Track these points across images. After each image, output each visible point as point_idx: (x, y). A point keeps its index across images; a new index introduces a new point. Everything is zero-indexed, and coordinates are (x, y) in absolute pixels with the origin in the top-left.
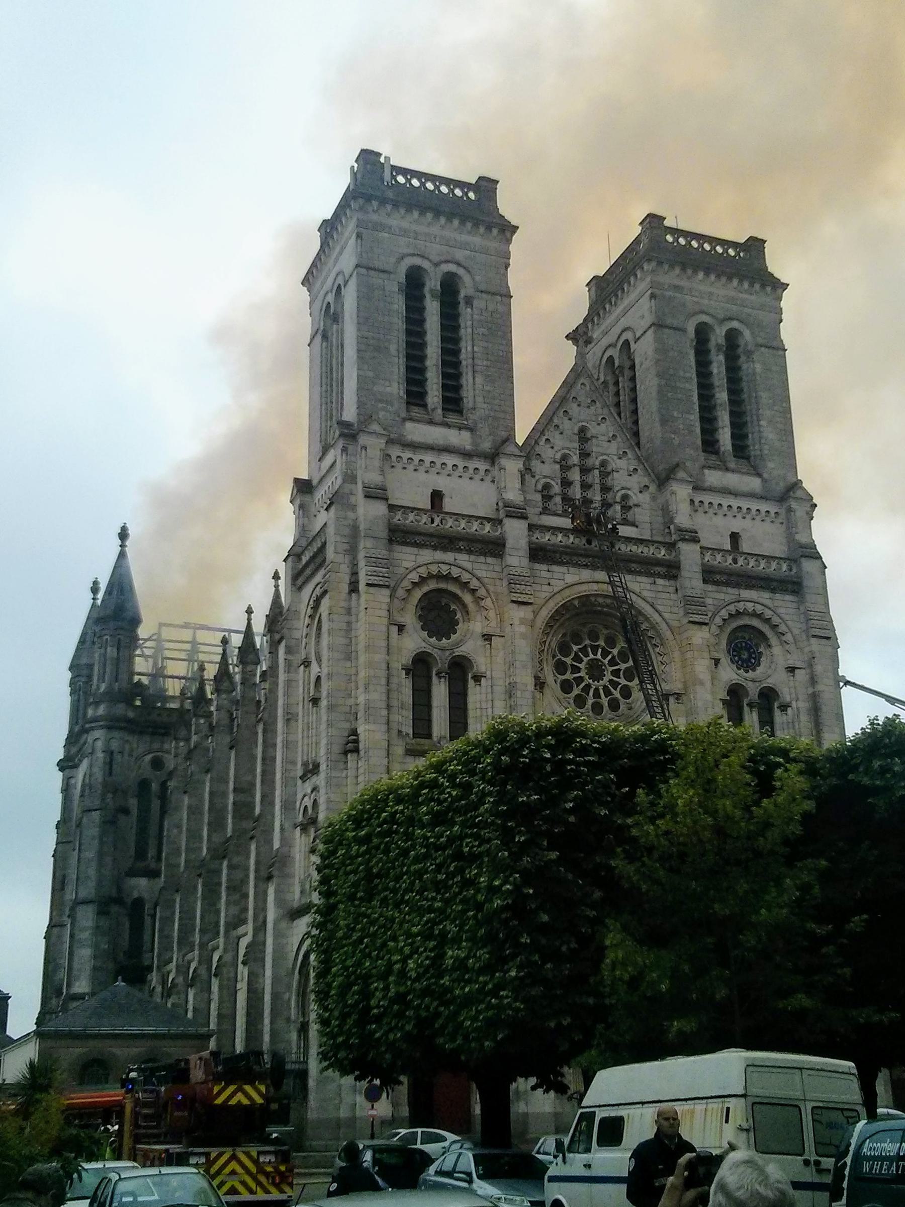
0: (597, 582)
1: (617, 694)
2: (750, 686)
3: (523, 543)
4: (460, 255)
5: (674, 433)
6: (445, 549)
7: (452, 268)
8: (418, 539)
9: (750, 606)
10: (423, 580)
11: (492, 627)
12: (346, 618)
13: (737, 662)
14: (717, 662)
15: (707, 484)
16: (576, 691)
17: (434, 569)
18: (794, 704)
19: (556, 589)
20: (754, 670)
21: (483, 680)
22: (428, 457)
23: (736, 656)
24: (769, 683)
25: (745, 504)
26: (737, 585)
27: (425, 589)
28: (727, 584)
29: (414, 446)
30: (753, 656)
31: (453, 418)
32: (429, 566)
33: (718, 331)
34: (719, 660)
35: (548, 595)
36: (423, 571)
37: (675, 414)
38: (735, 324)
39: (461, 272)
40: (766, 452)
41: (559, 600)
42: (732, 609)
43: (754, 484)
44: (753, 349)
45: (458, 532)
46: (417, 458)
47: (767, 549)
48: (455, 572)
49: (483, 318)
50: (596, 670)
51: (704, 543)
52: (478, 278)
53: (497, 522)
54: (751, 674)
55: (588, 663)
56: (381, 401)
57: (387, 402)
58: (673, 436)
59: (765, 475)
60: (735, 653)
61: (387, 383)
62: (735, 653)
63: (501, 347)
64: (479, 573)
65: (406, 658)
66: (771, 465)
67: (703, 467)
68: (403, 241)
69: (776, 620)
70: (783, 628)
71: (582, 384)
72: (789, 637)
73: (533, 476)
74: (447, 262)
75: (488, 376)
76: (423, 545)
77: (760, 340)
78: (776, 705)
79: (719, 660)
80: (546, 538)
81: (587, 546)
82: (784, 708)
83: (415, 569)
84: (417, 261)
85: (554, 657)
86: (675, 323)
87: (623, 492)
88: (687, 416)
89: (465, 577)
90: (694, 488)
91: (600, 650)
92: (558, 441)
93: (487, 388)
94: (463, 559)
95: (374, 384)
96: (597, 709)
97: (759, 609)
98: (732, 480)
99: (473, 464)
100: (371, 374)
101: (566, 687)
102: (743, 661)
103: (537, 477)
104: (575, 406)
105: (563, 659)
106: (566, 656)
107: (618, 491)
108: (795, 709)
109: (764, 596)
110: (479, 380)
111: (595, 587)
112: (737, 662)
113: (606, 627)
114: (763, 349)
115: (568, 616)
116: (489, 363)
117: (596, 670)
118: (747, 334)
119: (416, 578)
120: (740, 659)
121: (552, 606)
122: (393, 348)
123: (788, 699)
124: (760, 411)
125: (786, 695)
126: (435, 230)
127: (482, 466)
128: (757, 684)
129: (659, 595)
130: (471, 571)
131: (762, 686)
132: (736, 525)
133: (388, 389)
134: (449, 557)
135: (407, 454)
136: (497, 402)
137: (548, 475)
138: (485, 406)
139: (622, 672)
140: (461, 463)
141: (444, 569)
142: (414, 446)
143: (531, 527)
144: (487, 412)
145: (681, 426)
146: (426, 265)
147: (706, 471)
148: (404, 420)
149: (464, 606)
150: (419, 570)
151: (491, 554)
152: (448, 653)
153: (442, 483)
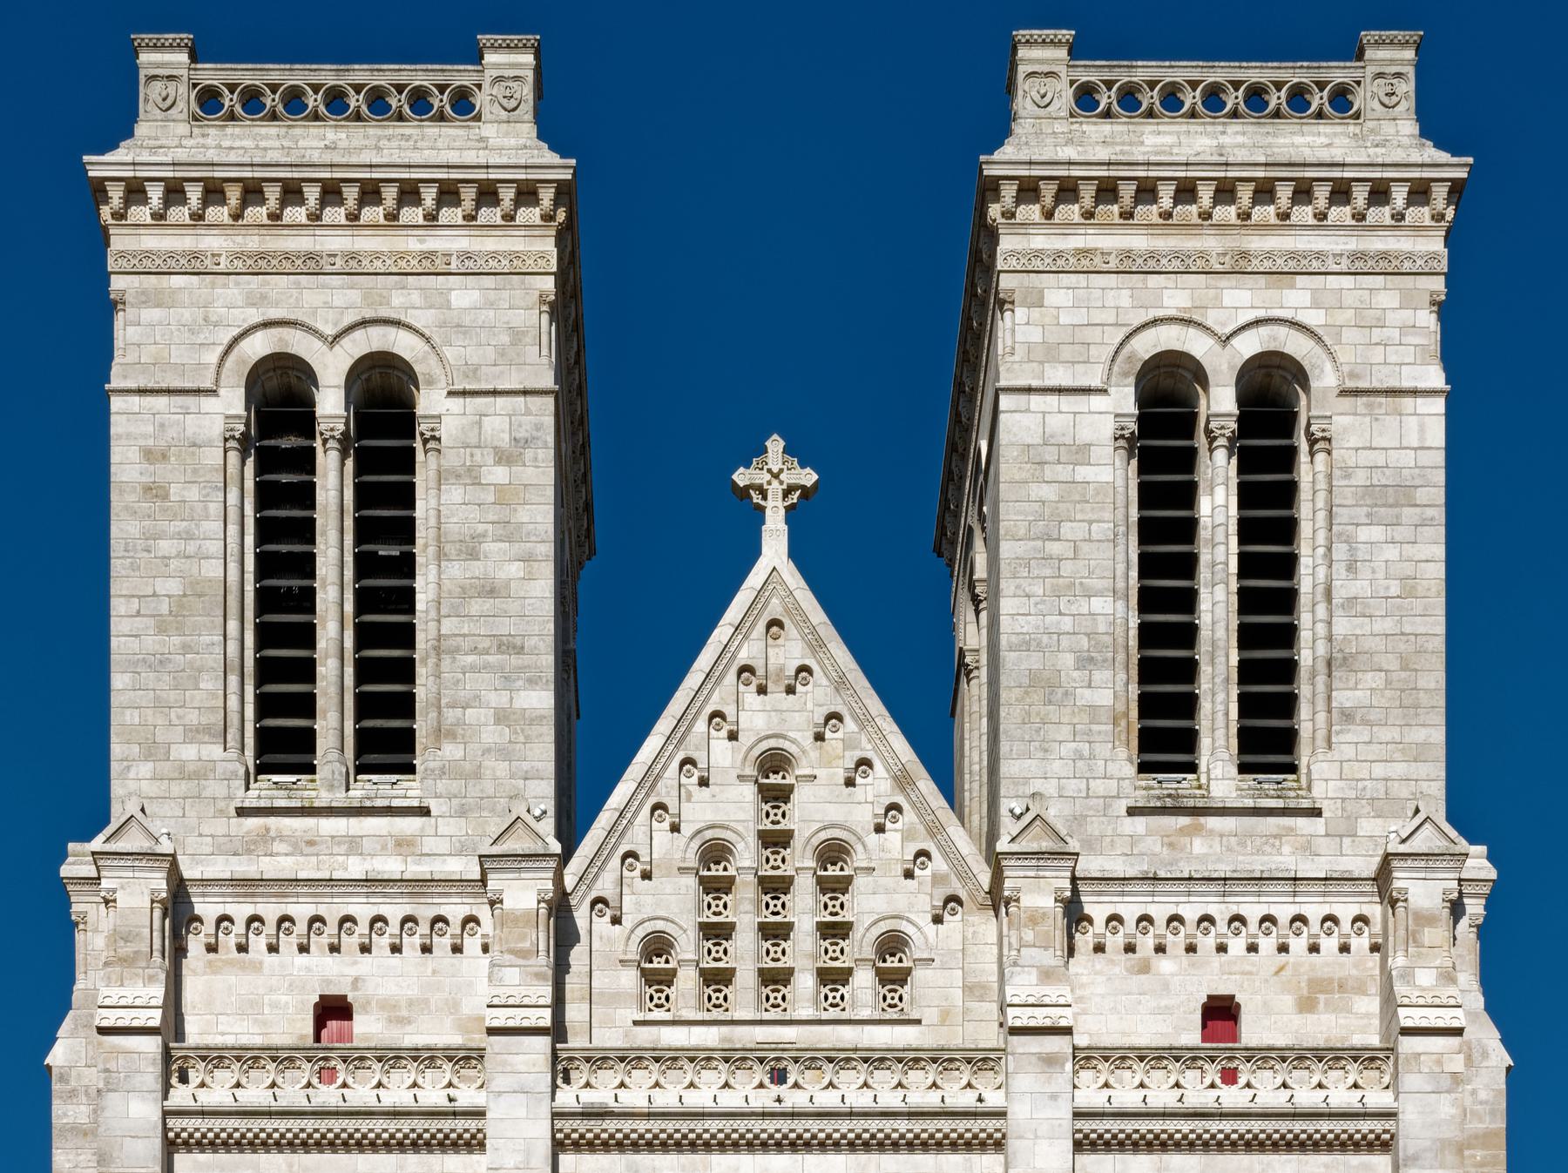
68: (233, 290)
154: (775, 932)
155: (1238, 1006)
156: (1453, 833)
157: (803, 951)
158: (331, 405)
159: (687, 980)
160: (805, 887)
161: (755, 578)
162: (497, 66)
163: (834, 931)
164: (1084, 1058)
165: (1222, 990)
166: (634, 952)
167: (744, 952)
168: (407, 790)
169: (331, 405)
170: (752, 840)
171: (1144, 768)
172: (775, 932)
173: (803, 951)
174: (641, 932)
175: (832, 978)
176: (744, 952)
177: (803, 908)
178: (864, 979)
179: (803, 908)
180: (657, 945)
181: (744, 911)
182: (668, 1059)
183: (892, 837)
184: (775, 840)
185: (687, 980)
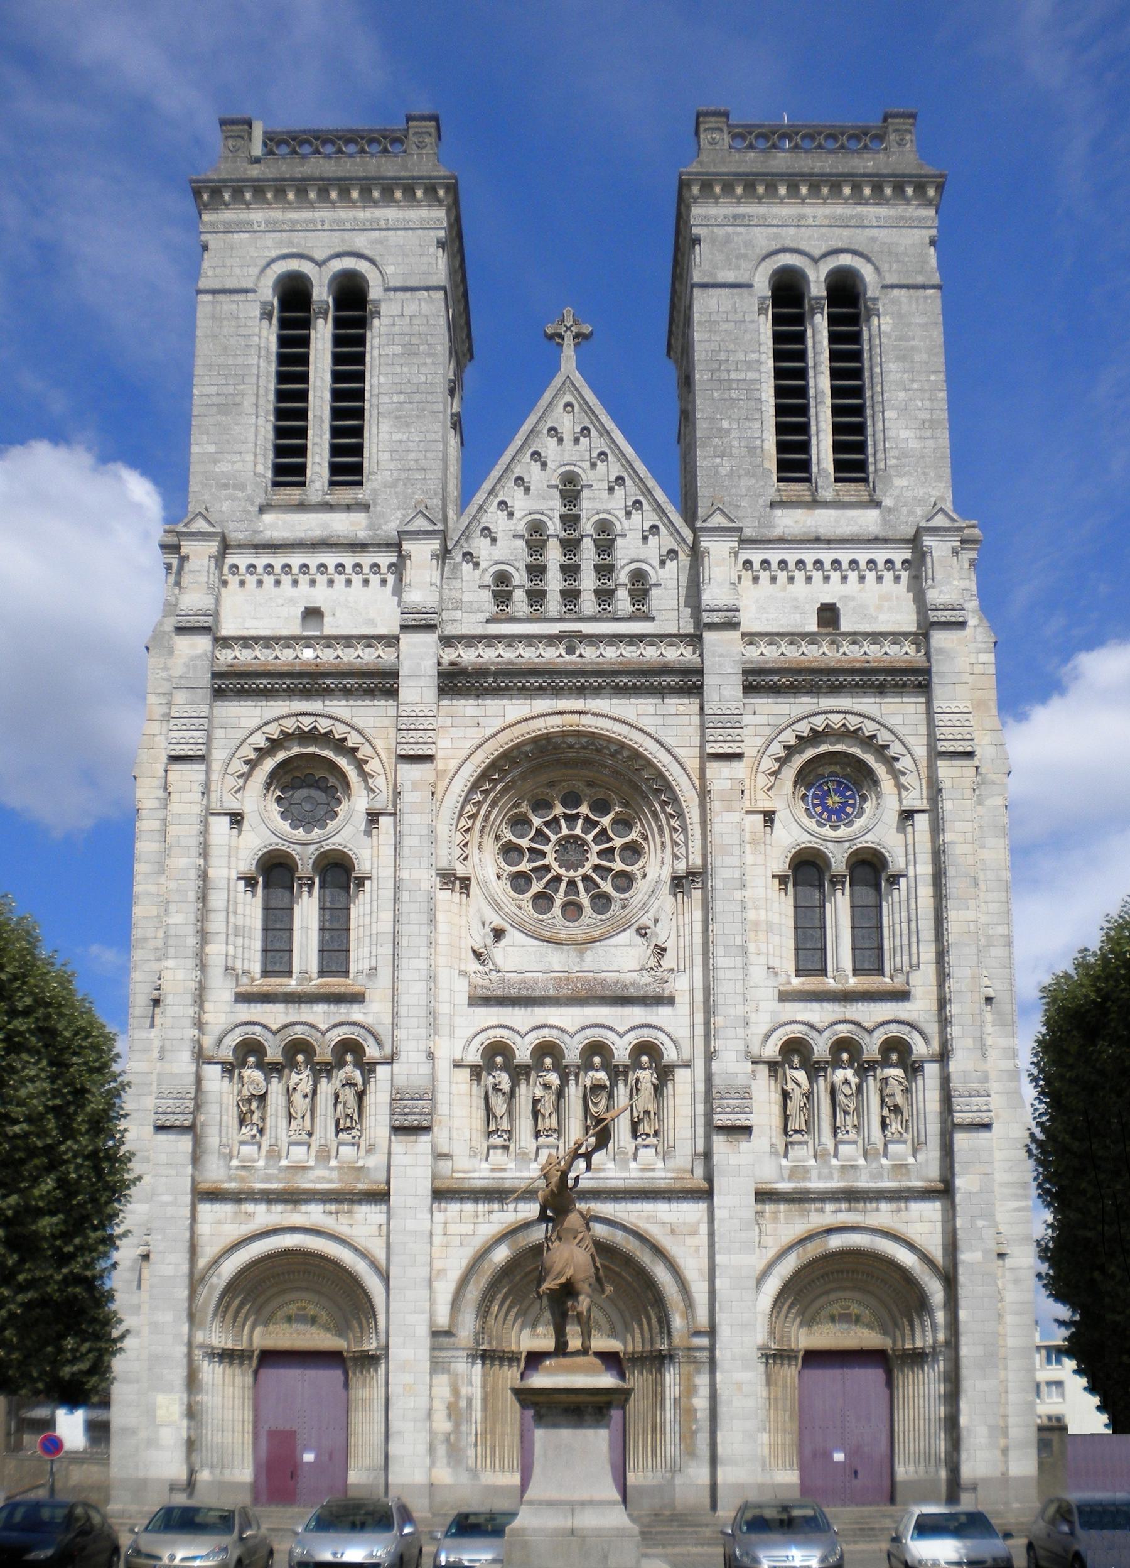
0: (561, 713)
1: (607, 887)
2: (830, 850)
3: (429, 668)
4: (360, 242)
5: (722, 456)
6: (307, 693)
7: (349, 263)
8: (263, 683)
9: (836, 720)
10: (275, 745)
11: (383, 801)
12: (161, 814)
13: (820, 815)
14: (769, 817)
15: (777, 532)
16: (537, 887)
17: (290, 725)
18: (911, 873)
19: (489, 732)
20: (850, 824)
21: (367, 883)
22: (296, 561)
23: (817, 805)
24: (869, 840)
25: (845, 556)
26: (813, 690)
27: (281, 756)
28: (793, 690)
29: (273, 547)
30: (851, 802)
31: (345, 495)
32: (281, 722)
33: (811, 275)
34: (774, 812)
35: (477, 742)
36: (274, 731)
37: (725, 424)
38: (845, 260)
39: (362, 266)
40: (892, 462)
41: (494, 749)
42: (804, 728)
43: (868, 521)
44: (877, 294)
45: (350, 664)
46: (278, 562)
47: (886, 623)
48: (323, 725)
49: (397, 329)
50: (572, 848)
51: (744, 628)
52: (389, 270)
53: (391, 641)
54: (843, 832)
55: (558, 843)
56: (226, 486)
57: (235, 487)
58: (718, 460)
59: (887, 502)
60: (815, 801)
61: (237, 458)
62: (815, 801)
63: (423, 370)
64: (359, 723)
65: (247, 863)
66: (899, 482)
67: (773, 505)
68: (270, 239)
69: (883, 737)
70: (895, 749)
71: (569, 404)
72: (904, 763)
73: (476, 565)
74: (339, 255)
75: (397, 417)
76: (270, 691)
77: (890, 279)
78: (884, 876)
79: (774, 812)
80: (468, 656)
81: (567, 658)
82: (894, 880)
83: (260, 728)
84: (294, 265)
85: (497, 838)
86: (730, 276)
87: (633, 566)
88: (748, 424)
89: (339, 731)
90: (741, 541)
91: (562, 822)
92: (520, 502)
93: (397, 437)
94: (338, 707)
95: (215, 462)
96: (572, 909)
97: (853, 722)
98: (823, 521)
99: (366, 560)
100: (211, 449)
101: (520, 881)
102: (831, 812)
103: (483, 564)
104: (552, 442)
105: (515, 840)
106: (522, 836)
107: (622, 567)
108: (912, 880)
109: (867, 704)
110: (385, 427)
111: (556, 720)
112: (820, 815)
113: (590, 784)
114: (896, 292)
115: (516, 772)
116: (402, 398)
117: (572, 848)
118: (867, 272)
119: (260, 740)
120: (845, 804)
121: (481, 760)
122: (248, 403)
123: (902, 865)
124: (885, 395)
125: (897, 862)
126: (323, 214)
127: (386, 559)
128: (847, 845)
129: (669, 721)
130: (348, 720)
131: (855, 848)
132: (831, 592)
133: (236, 467)
134: (315, 706)
135: (261, 561)
136: (413, 456)
137: (503, 559)
138: (392, 465)
139: (617, 853)
140: (348, 560)
141: (306, 723)
142: (273, 547)
143: (447, 641)
144: (395, 474)
145: (736, 443)
146: (306, 267)
147: (778, 512)
148: (262, 510)
149: (343, 776)
150: (265, 729)
151: (380, 690)
152: (312, 848)
153: (320, 596)
154: (570, 571)
155: (838, 609)
156: (955, 516)
157: (588, 582)
158: (322, 294)
159: (519, 595)
160: (587, 545)
161: (558, 380)
162: (416, 127)
163: (605, 570)
164: (751, 638)
165: (828, 600)
166: (488, 580)
167: (554, 582)
168: (361, 494)
169: (322, 294)
170: (557, 520)
171: (780, 480)
172: (570, 571)
173: (588, 582)
174: (492, 570)
175: (604, 595)
176: (554, 582)
177: (588, 554)
178: (622, 594)
179: (588, 554)
180: (502, 578)
181: (554, 555)
182: (511, 640)
183: (636, 516)
184: (570, 521)
185: (519, 595)
